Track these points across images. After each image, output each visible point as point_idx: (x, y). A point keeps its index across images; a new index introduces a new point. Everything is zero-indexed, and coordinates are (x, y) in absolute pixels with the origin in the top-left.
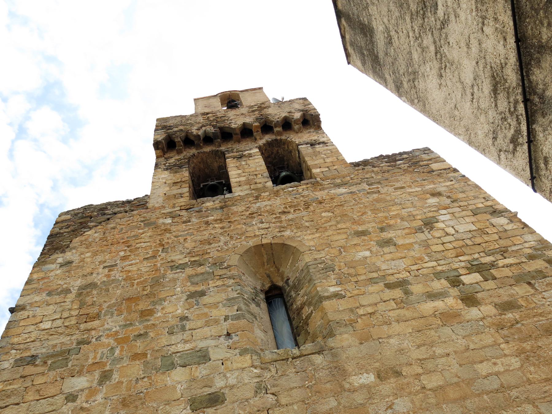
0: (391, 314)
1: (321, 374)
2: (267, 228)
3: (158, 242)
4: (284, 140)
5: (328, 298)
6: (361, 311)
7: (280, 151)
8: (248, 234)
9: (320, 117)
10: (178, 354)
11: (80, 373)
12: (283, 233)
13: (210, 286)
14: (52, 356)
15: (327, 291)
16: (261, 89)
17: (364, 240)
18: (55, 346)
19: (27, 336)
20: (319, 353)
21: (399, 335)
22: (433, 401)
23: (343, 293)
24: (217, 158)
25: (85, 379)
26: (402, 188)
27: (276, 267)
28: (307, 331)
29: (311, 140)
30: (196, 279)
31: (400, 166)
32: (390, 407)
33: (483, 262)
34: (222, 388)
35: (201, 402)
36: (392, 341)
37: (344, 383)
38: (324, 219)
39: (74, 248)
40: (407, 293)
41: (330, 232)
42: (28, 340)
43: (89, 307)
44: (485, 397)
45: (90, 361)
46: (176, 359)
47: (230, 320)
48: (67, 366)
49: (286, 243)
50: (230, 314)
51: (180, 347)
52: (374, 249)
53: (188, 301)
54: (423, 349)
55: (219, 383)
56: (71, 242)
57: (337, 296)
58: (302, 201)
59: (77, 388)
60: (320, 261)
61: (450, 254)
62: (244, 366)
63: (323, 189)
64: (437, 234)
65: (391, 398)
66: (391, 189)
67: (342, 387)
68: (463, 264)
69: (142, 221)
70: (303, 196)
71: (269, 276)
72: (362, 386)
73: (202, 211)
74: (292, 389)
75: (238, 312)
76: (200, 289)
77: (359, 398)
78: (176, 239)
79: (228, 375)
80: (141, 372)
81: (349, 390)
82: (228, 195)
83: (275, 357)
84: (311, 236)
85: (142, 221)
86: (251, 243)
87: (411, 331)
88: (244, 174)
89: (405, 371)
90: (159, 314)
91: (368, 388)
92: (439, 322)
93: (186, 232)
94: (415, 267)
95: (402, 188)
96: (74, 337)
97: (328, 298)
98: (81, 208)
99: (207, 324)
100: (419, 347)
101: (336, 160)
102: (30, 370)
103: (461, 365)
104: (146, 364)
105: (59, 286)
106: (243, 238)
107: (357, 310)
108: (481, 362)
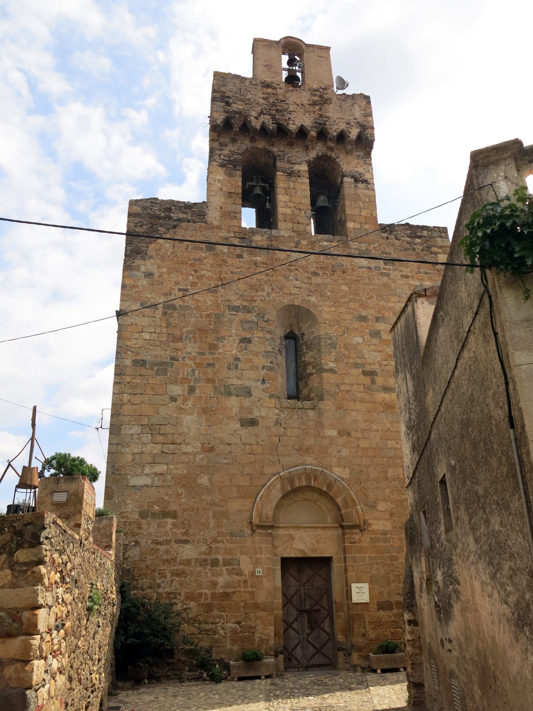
0: (359, 395)
1: (311, 423)
2: (299, 288)
3: (218, 275)
4: (334, 158)
5: (327, 371)
6: (343, 388)
7: (325, 165)
9: (375, 142)
10: (234, 387)
11: (175, 382)
13: (254, 335)
14: (156, 364)
15: (327, 364)
16: (328, 49)
17: (363, 326)
18: (156, 357)
19: (135, 341)
20: (312, 409)
21: (358, 411)
22: (360, 454)
23: (336, 369)
24: (267, 156)
25: (180, 388)
26: (407, 277)
27: (298, 321)
28: (306, 382)
29: (357, 172)
30: (246, 326)
31: (415, 247)
32: (339, 452)
34: (257, 417)
35: (245, 422)
36: (353, 413)
37: (321, 432)
38: (342, 293)
39: (151, 257)
40: (373, 382)
41: (342, 310)
42: (137, 346)
43: (173, 328)
44: (384, 459)
45: (181, 376)
46: (232, 390)
47: (265, 370)
48: (167, 375)
49: (310, 309)
50: (266, 365)
51: (235, 381)
52: (366, 338)
53: (240, 344)
54: (366, 423)
55: (256, 414)
56: (148, 247)
57: (332, 371)
58: (331, 263)
59: (176, 393)
60: (329, 337)
62: (271, 406)
65: (341, 447)
66: (399, 274)
67: (319, 434)
71: (291, 326)
72: (330, 437)
74: (294, 428)
75: (271, 365)
76: (248, 337)
77: (326, 442)
78: (231, 275)
79: (262, 410)
80: (212, 393)
81: (322, 437)
82: (274, 232)
83: (288, 405)
84: (329, 308)
86: (286, 301)
87: (365, 410)
88: (290, 204)
89: (353, 434)
90: (221, 350)
91: (331, 438)
92: (382, 409)
93: (239, 270)
94: (385, 363)
95: (407, 277)
96: (167, 353)
97: (327, 371)
98: (148, 199)
99: (251, 368)
100: (365, 421)
101: (370, 215)
102: (143, 371)
103: (381, 439)
104: (215, 388)
105: (148, 299)
106: (281, 293)
107: (341, 386)
108: (392, 440)
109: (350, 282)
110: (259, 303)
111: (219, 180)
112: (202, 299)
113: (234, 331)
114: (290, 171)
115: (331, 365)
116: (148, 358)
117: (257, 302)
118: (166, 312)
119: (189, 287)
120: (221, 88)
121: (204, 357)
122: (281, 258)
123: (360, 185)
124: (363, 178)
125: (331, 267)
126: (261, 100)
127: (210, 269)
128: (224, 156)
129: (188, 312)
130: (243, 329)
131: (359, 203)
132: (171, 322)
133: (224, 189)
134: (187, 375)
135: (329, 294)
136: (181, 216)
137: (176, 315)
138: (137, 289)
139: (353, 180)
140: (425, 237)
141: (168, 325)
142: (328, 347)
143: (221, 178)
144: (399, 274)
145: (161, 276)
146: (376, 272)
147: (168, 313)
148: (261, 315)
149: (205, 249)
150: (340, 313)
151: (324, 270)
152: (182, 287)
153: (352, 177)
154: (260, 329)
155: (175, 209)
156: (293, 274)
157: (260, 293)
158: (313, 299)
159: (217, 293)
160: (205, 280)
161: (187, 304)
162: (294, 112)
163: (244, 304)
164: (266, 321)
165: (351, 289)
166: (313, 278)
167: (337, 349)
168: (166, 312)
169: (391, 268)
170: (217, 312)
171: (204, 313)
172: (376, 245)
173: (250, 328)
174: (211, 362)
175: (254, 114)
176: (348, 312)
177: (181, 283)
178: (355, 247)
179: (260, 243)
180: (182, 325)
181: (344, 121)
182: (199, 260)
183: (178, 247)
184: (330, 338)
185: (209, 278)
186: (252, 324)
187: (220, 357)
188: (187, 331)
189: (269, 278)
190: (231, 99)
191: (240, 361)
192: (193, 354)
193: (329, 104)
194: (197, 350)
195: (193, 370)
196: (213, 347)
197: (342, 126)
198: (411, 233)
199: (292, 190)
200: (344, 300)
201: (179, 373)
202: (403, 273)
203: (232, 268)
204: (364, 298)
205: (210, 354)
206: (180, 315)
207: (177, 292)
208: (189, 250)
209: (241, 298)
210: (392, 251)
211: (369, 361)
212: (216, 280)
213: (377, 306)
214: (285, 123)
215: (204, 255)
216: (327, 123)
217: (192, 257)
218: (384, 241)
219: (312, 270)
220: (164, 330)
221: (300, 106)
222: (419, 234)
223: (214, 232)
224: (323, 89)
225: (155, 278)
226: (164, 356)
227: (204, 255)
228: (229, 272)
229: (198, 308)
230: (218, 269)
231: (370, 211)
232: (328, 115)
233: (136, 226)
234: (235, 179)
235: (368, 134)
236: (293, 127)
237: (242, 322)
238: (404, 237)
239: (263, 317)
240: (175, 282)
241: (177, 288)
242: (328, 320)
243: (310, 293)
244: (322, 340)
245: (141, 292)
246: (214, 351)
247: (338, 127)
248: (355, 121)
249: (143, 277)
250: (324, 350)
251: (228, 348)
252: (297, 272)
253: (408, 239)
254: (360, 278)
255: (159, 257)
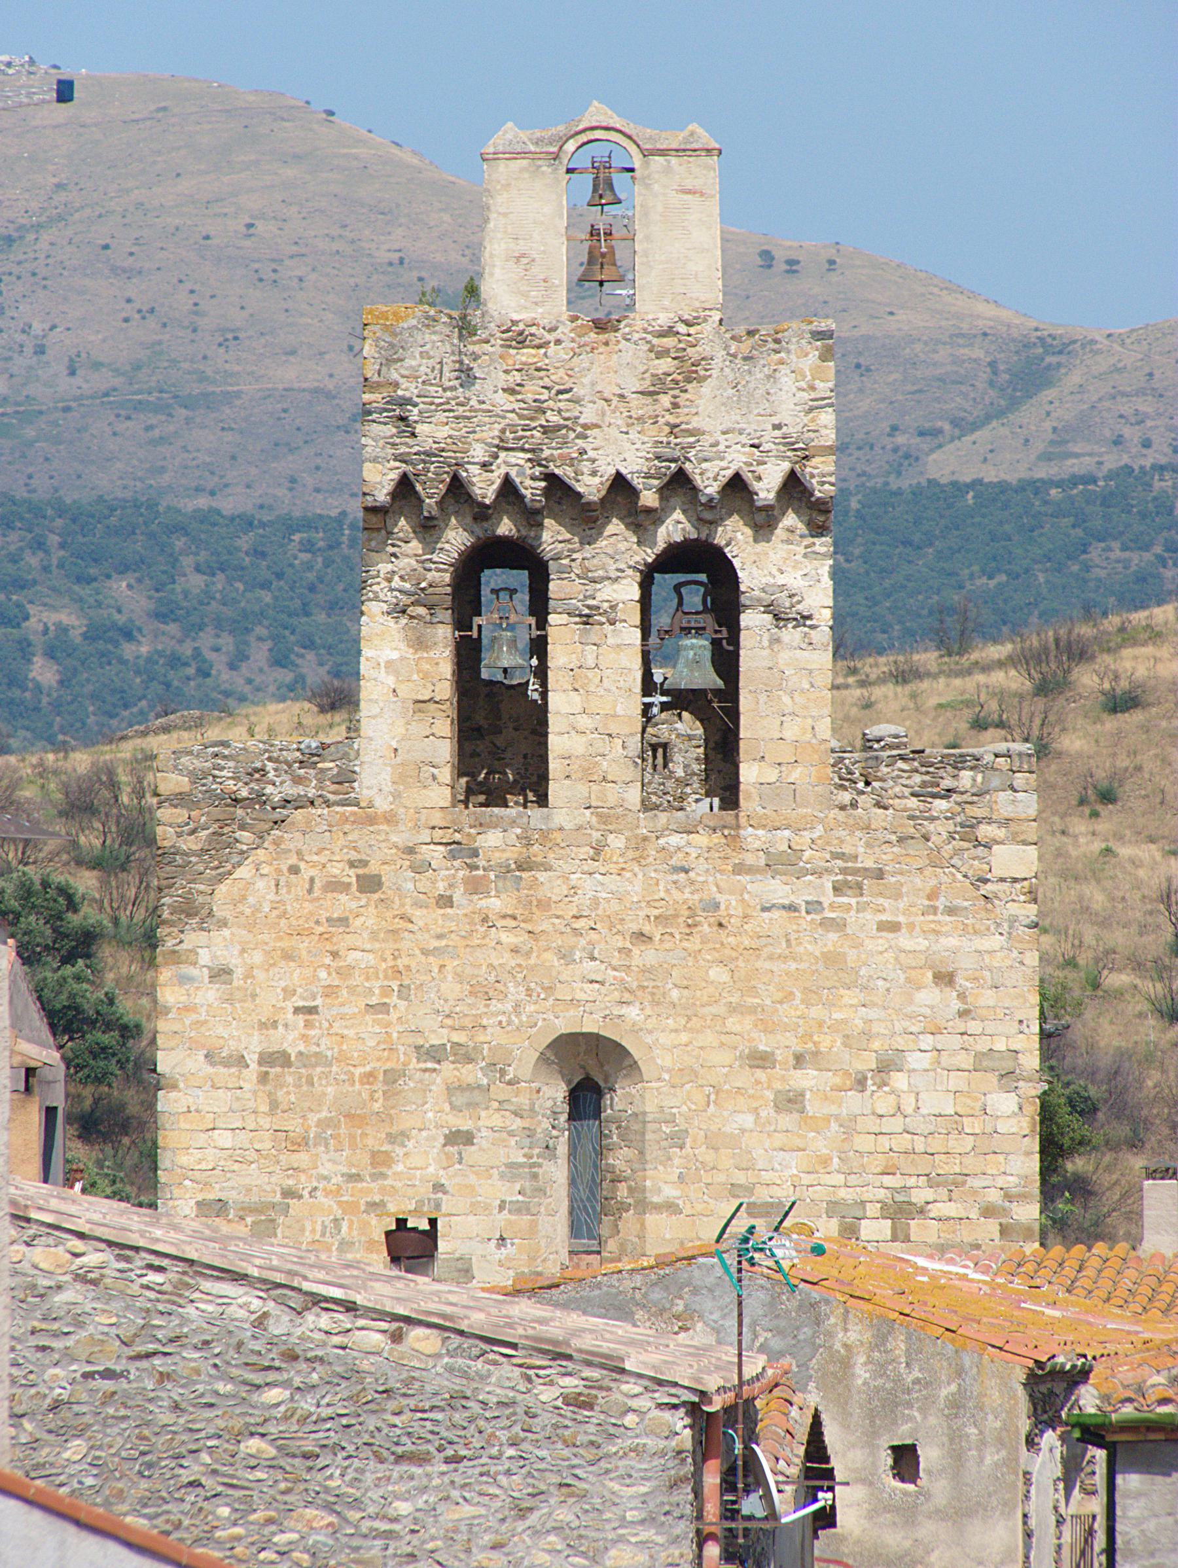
8: (563, 993)
12: (624, 1010)
13: (481, 1123)
15: (660, 1191)
17: (758, 1082)
18: (249, 1190)
19: (198, 1154)
23: (680, 1202)
26: (894, 927)
30: (459, 1100)
33: (914, 1200)
38: (711, 989)
39: (223, 923)
42: (203, 1166)
50: (508, 1199)
52: (763, 1114)
53: (448, 1148)
57: (671, 1207)
60: (668, 1117)
61: (878, 1163)
63: (739, 869)
64: (884, 1104)
68: (882, 1194)
69: (352, 864)
70: (692, 883)
73: (477, 868)
75: (520, 1198)
76: (465, 1128)
82: (535, 812)
85: (352, 864)
88: (584, 722)
90: (400, 1168)
94: (807, 1179)
95: (894, 927)
96: (273, 1180)
97: (658, 1208)
99: (474, 1210)
101: (809, 736)
105: (221, 1042)
106: (551, 1001)
109: (734, 954)
110: (492, 1036)
111: (389, 664)
112: (350, 1033)
113: (430, 1115)
114: (588, 607)
115: (670, 1192)
116: (231, 1196)
117: (489, 1030)
118: (267, 1073)
119: (318, 1002)
120: (384, 369)
121: (359, 1185)
122: (554, 898)
123: (791, 635)
124: (799, 607)
125: (687, 913)
126: (502, 399)
127: (368, 947)
128: (401, 577)
129: (319, 1069)
130: (453, 1107)
131: (779, 697)
132: (280, 1099)
133: (404, 691)
134: (323, 1235)
135: (675, 994)
136: (291, 790)
137: (290, 1079)
138: (194, 1016)
139: (769, 617)
140: (962, 793)
141: (274, 1105)
142: (664, 1144)
143: (395, 655)
144: (871, 918)
145: (249, 975)
146: (809, 918)
147: (271, 1076)
148: (497, 1068)
149: (354, 887)
150: (701, 1048)
151: (665, 926)
152: (301, 1004)
153: (769, 608)
154: (495, 1105)
155: (276, 770)
156: (583, 942)
157: (495, 1006)
158: (632, 1013)
159: (388, 1013)
160: (357, 979)
161: (315, 1049)
162: (597, 426)
163: (458, 1037)
164: (510, 1083)
165: (736, 974)
166: (636, 951)
167: (688, 1150)
168: (267, 1073)
169: (853, 901)
170: (388, 1066)
171: (358, 1071)
172: (819, 831)
173: (469, 1105)
174: (377, 1199)
175: (479, 453)
176: (722, 1044)
177: (300, 990)
178: (758, 844)
179: (497, 855)
180: (306, 1105)
181: (744, 439)
182: (343, 921)
183: (288, 885)
184: (672, 1121)
185: (370, 973)
186: (476, 1092)
187: (399, 1185)
188: (319, 1120)
189: (519, 961)
190: (415, 405)
191: (445, 1193)
192: (334, 1181)
193: (701, 380)
194: (345, 1170)
195: (336, 1220)
196: (381, 1160)
197: (736, 460)
198: (924, 784)
199: (590, 674)
200: (713, 1010)
201: (302, 1230)
202: (884, 917)
203: (427, 936)
204: (768, 1002)
205: (375, 1177)
206: (300, 1078)
207: (290, 1016)
208: (317, 893)
209: (449, 1022)
210: (861, 850)
211: (766, 1176)
212: (386, 977)
213: (801, 1022)
214: (570, 471)
215: (354, 905)
216: (691, 454)
217: (324, 915)
218: (841, 815)
219: (635, 927)
220: (265, 1122)
221: (615, 400)
222: (947, 783)
223: (378, 832)
224: (688, 324)
225: (235, 983)
226: (268, 1188)
227: (354, 905)
228: (418, 952)
229: (342, 1058)
230: (391, 945)
231: (810, 721)
232: (695, 423)
233: (179, 835)
234: (431, 654)
235: (812, 476)
236: (591, 487)
237: (451, 1090)
238: (903, 797)
239: (503, 1072)
240: (284, 990)
241: (289, 1006)
242: (669, 1071)
243: (627, 997)
244: (650, 1126)
245: (206, 1022)
246: (384, 1170)
247: (724, 464)
248: (777, 433)
249: (207, 980)
250: (652, 1153)
251: (416, 1161)
252: (593, 935)
253: (913, 802)
254: (763, 941)
255: (242, 919)
